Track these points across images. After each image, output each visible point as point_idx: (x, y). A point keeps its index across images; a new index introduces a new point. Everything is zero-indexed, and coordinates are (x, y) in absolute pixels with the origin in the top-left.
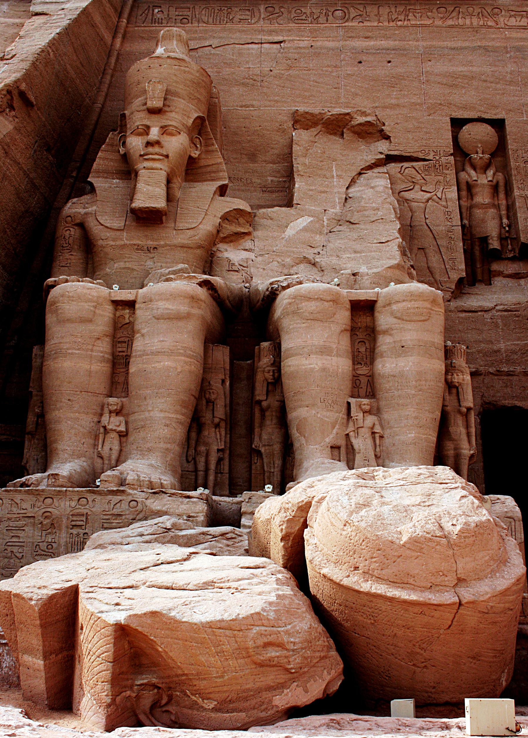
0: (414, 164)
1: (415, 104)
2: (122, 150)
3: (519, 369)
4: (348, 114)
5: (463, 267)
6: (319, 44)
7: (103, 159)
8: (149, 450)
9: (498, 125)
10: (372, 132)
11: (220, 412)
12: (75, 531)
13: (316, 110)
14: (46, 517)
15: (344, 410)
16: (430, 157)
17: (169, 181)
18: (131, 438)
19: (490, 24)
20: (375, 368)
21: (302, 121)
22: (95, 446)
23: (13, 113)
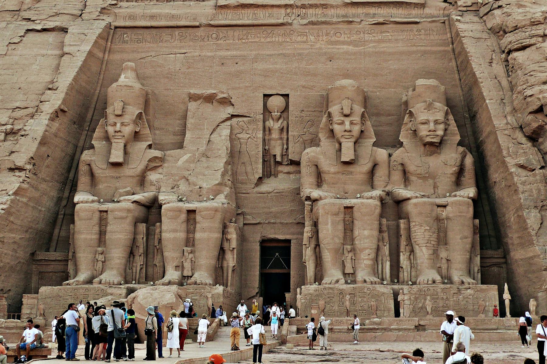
0: (245, 119)
1: (247, 87)
3: (278, 221)
5: (261, 171)
6: (204, 54)
7: (98, 133)
8: (112, 268)
10: (226, 102)
11: (141, 250)
15: (182, 253)
16: (252, 116)
17: (125, 146)
18: (107, 263)
19: (288, 40)
20: (196, 235)
22: (94, 266)
23: (58, 119)
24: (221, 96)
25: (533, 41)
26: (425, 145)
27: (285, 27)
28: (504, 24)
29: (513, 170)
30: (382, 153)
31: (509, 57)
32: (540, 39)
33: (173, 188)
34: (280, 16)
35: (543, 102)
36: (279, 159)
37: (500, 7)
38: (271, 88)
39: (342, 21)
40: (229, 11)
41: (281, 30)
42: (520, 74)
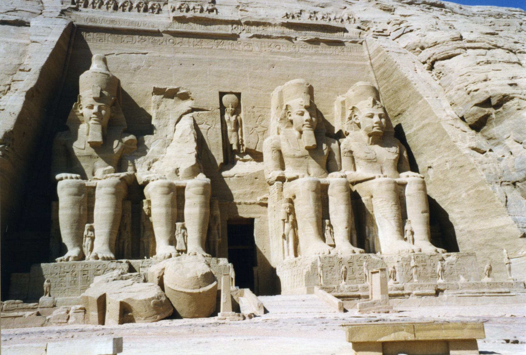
3: (243, 201)
4: (176, 89)
6: (163, 55)
9: (238, 95)
13: (162, 87)
16: (210, 109)
19: (236, 48)
24: (182, 91)
25: (457, 51)
32: (464, 50)
33: (149, 169)
35: (491, 94)
36: (235, 147)
37: (411, 31)
38: (224, 87)
41: (231, 42)
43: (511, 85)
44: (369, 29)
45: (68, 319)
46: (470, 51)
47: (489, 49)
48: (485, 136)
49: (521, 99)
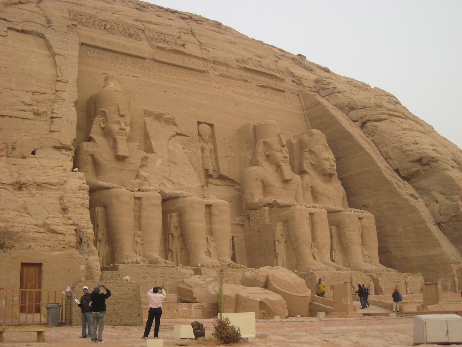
2: (102, 125)
4: (163, 113)
9: (211, 125)
12: (162, 278)
13: (152, 110)
14: (153, 274)
16: (191, 136)
19: (208, 84)
21: (147, 113)
24: (167, 116)
25: (386, 117)
26: (324, 175)
27: (206, 74)
28: (351, 103)
29: (408, 197)
30: (298, 177)
31: (368, 124)
32: (389, 116)
34: (200, 65)
35: (423, 155)
37: (339, 92)
39: (241, 79)
40: (164, 53)
42: (387, 136)
43: (433, 150)
44: (302, 84)
45: (190, 314)
46: (394, 119)
47: (405, 119)
48: (414, 186)
49: (442, 162)
